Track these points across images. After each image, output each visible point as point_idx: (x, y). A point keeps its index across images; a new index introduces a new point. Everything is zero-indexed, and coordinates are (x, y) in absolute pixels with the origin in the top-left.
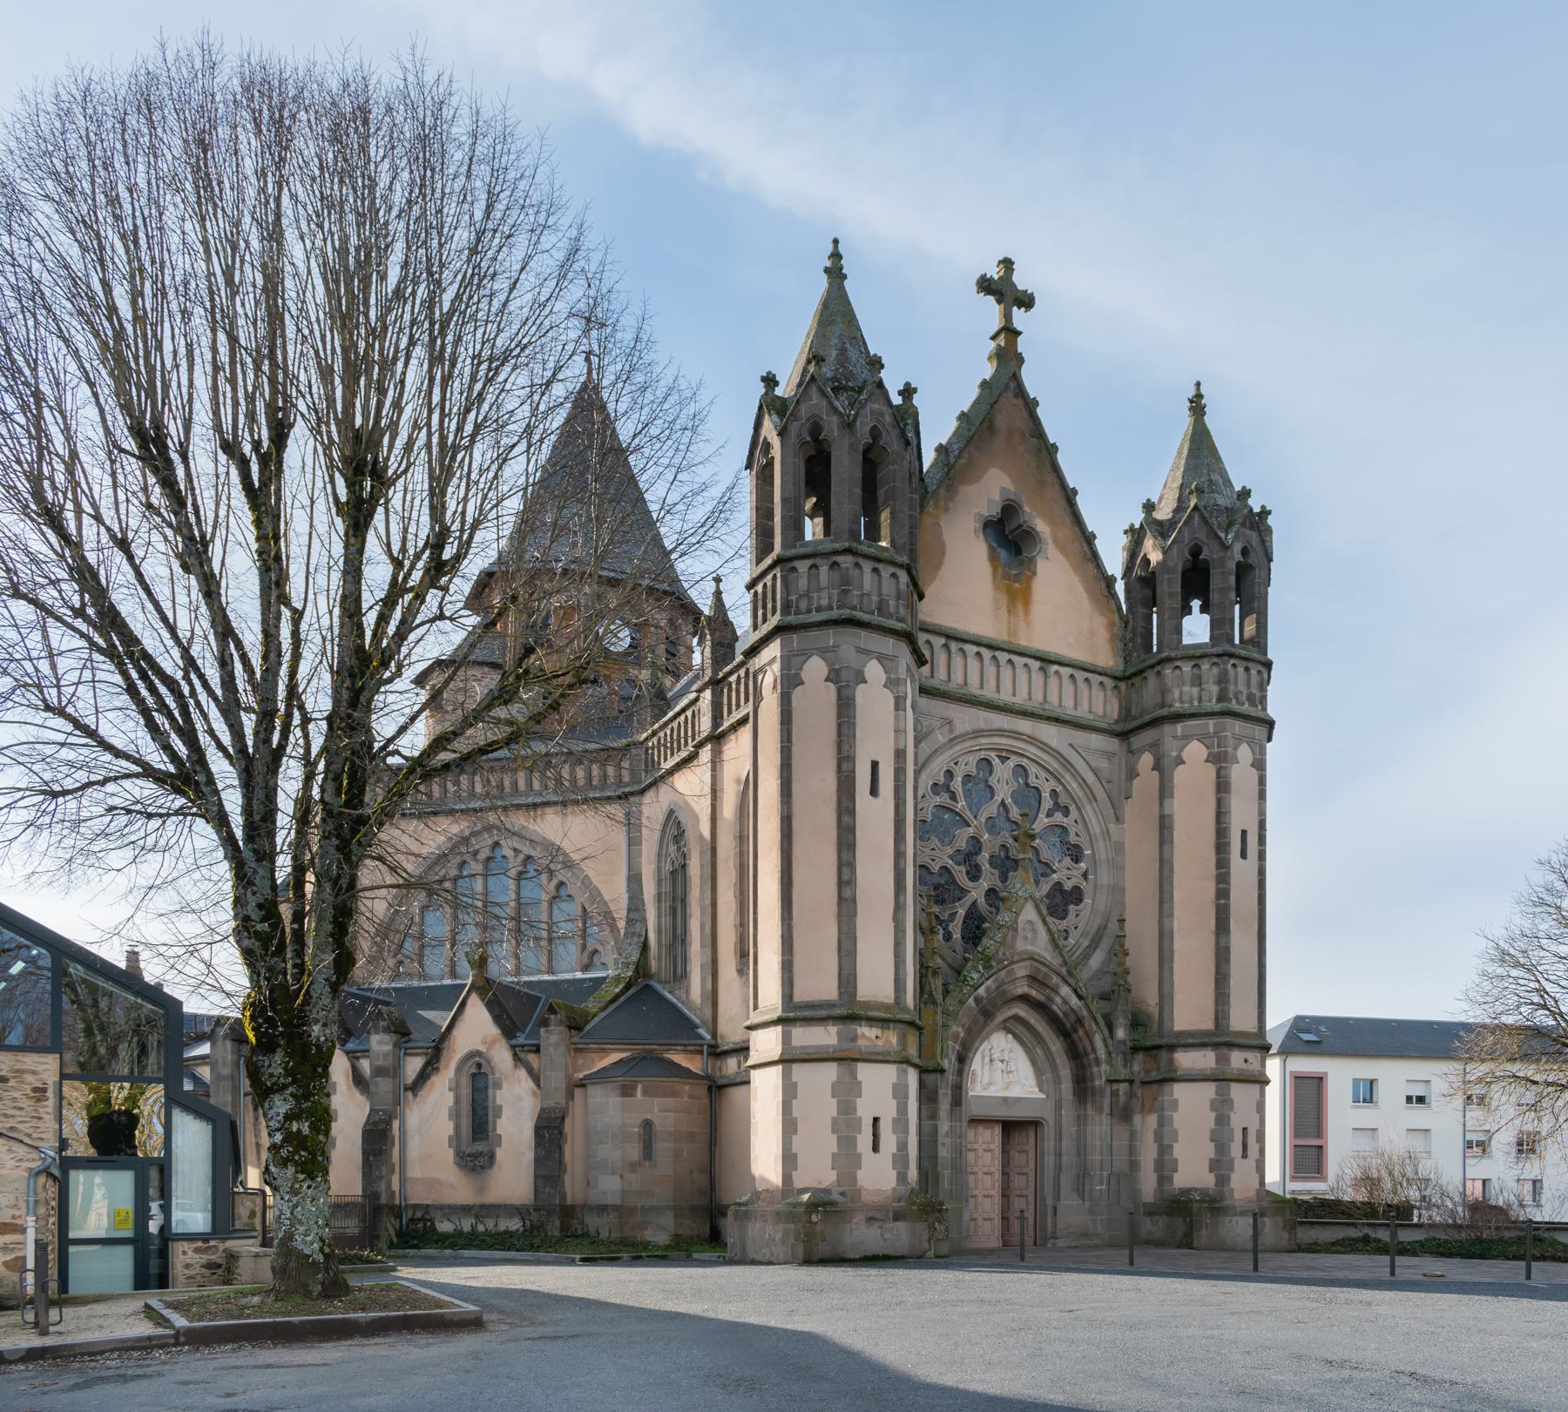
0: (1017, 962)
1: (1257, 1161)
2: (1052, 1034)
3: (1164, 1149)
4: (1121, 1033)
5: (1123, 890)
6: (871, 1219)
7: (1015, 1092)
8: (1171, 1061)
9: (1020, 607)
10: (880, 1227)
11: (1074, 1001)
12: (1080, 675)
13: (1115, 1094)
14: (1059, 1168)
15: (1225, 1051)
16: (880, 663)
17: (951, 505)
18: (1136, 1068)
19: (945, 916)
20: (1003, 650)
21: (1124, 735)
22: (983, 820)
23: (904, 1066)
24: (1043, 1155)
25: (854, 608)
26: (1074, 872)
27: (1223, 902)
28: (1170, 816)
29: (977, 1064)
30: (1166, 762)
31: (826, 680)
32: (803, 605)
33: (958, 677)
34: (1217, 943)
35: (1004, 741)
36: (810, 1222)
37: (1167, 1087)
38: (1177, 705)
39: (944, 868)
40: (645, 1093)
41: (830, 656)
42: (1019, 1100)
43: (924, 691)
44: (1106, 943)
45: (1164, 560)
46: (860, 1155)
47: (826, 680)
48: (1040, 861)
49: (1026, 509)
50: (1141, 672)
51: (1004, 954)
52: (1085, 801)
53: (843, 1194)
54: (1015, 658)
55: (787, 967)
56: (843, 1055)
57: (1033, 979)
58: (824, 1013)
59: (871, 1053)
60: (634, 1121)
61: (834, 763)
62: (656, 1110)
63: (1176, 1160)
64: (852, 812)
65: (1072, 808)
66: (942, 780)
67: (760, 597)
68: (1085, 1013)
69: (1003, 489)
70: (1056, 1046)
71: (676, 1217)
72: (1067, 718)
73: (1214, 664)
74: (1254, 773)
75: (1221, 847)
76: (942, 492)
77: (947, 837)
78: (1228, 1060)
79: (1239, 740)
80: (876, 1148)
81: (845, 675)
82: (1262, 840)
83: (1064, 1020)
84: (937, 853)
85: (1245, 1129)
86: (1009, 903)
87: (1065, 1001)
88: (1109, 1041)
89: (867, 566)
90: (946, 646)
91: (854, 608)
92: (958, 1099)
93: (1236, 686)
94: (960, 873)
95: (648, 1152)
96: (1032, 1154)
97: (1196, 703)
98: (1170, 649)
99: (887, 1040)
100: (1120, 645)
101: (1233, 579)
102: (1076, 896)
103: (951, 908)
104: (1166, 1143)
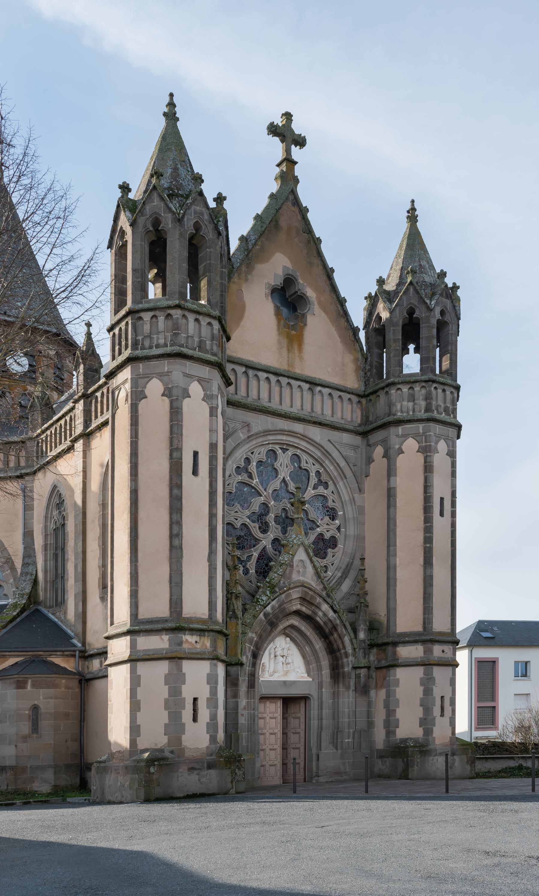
0: (293, 588)
1: (450, 718)
2: (316, 637)
3: (390, 713)
4: (362, 635)
5: (364, 538)
6: (192, 769)
7: (292, 677)
8: (395, 653)
9: (296, 347)
10: (198, 774)
11: (331, 614)
12: (336, 394)
13: (358, 676)
14: (321, 728)
15: (429, 645)
16: (200, 383)
17: (249, 277)
18: (372, 658)
19: (244, 558)
20: (284, 376)
21: (364, 434)
22: (270, 492)
23: (215, 661)
24: (310, 719)
25: (182, 346)
26: (331, 527)
27: (428, 545)
28: (395, 488)
29: (266, 659)
30: (392, 452)
31: (163, 395)
32: (147, 343)
33: (254, 394)
34: (425, 573)
36: (149, 773)
37: (392, 671)
38: (399, 414)
39: (244, 525)
40: (34, 686)
41: (165, 378)
42: (294, 682)
43: (230, 403)
44: (352, 574)
45: (391, 317)
46: (184, 724)
47: (163, 395)
48: (308, 519)
49: (300, 281)
50: (375, 392)
51: (284, 583)
52: (339, 479)
53: (172, 752)
54: (293, 382)
55: (134, 595)
56: (173, 655)
57: (303, 599)
58: (159, 626)
59: (192, 653)
60: (26, 705)
61: (168, 452)
62: (41, 697)
63: (398, 720)
64: (180, 486)
65: (330, 483)
66: (243, 464)
67: (117, 337)
68: (338, 622)
69: (285, 267)
70: (319, 645)
71: (55, 773)
72: (327, 422)
73: (423, 387)
74: (449, 460)
76: (244, 268)
77: (245, 503)
78: (431, 651)
79: (439, 438)
80: (195, 719)
81: (175, 392)
82: (453, 504)
83: (325, 627)
84: (239, 514)
85: (442, 697)
86: (287, 548)
87: (325, 615)
88: (354, 641)
89: (191, 317)
90: (245, 373)
91: (182, 346)
92: (252, 684)
93: (437, 401)
94: (255, 528)
95: (35, 727)
96: (302, 720)
97: (411, 413)
98: (394, 376)
99: (204, 642)
100: (362, 373)
101: (435, 331)
102: (333, 543)
103: (248, 552)
104: (391, 708)
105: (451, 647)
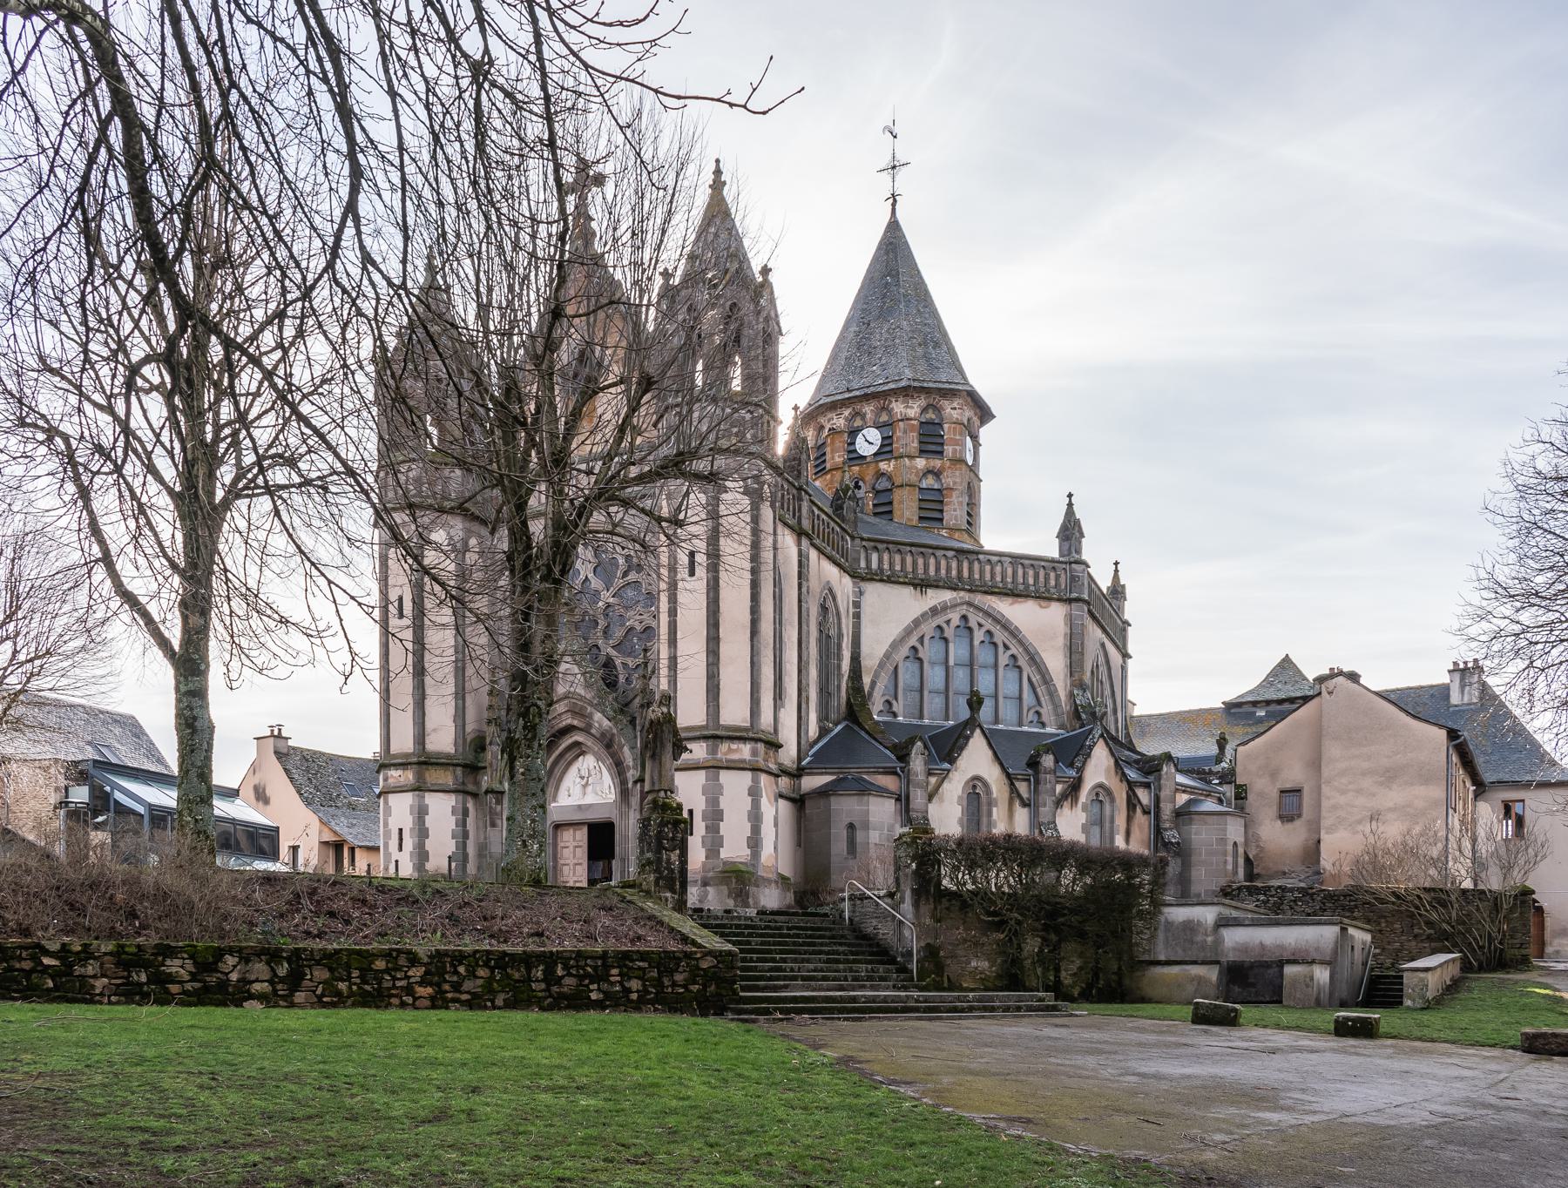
7: (590, 799)
11: (606, 723)
42: (591, 805)
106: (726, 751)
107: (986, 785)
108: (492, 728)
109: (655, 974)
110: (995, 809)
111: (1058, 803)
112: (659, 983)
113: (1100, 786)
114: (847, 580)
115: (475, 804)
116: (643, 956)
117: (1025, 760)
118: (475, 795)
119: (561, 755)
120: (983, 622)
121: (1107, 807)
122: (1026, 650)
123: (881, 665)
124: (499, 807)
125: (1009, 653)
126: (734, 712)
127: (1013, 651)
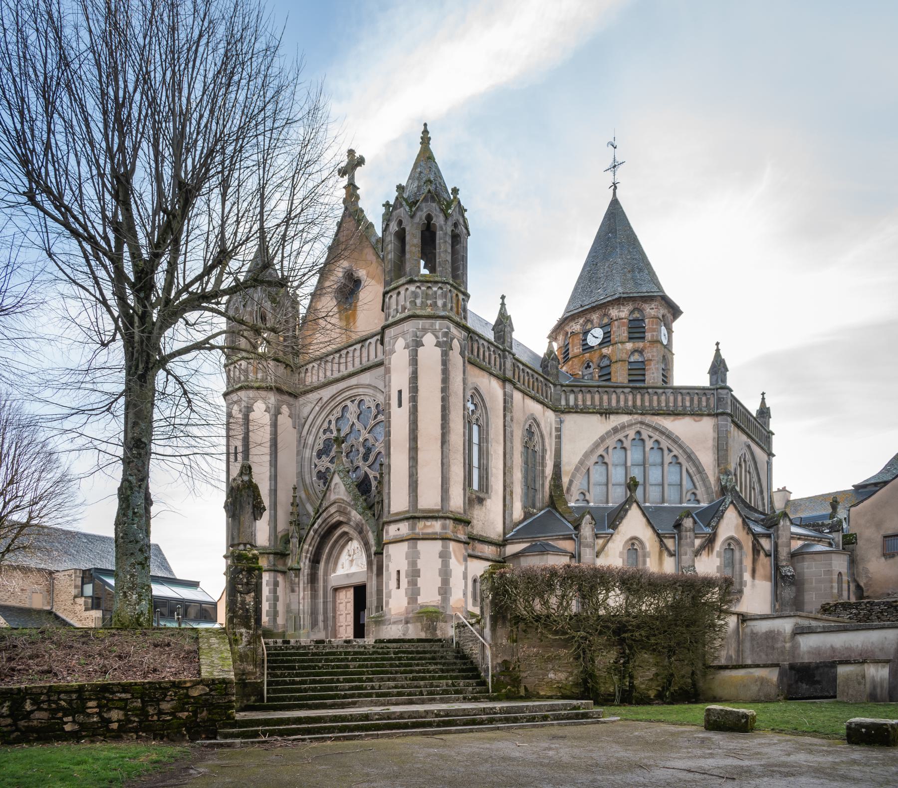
11: (359, 517)
35: (347, 393)
42: (354, 574)
75: (414, 399)
85: (398, 572)
105: (407, 524)
106: (422, 527)
107: (641, 542)
108: (293, 527)
109: (138, 703)
110: (648, 560)
111: (697, 553)
112: (143, 712)
113: (732, 538)
114: (550, 414)
115: (284, 579)
116: (125, 688)
117: (673, 523)
118: (284, 573)
119: (336, 541)
120: (652, 434)
121: (737, 554)
122: (685, 451)
123: (577, 469)
124: (297, 580)
125: (672, 454)
126: (429, 499)
127: (675, 452)
